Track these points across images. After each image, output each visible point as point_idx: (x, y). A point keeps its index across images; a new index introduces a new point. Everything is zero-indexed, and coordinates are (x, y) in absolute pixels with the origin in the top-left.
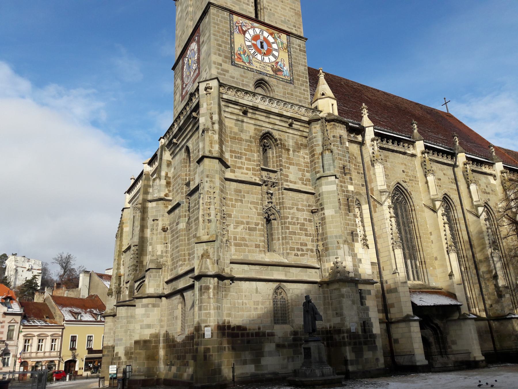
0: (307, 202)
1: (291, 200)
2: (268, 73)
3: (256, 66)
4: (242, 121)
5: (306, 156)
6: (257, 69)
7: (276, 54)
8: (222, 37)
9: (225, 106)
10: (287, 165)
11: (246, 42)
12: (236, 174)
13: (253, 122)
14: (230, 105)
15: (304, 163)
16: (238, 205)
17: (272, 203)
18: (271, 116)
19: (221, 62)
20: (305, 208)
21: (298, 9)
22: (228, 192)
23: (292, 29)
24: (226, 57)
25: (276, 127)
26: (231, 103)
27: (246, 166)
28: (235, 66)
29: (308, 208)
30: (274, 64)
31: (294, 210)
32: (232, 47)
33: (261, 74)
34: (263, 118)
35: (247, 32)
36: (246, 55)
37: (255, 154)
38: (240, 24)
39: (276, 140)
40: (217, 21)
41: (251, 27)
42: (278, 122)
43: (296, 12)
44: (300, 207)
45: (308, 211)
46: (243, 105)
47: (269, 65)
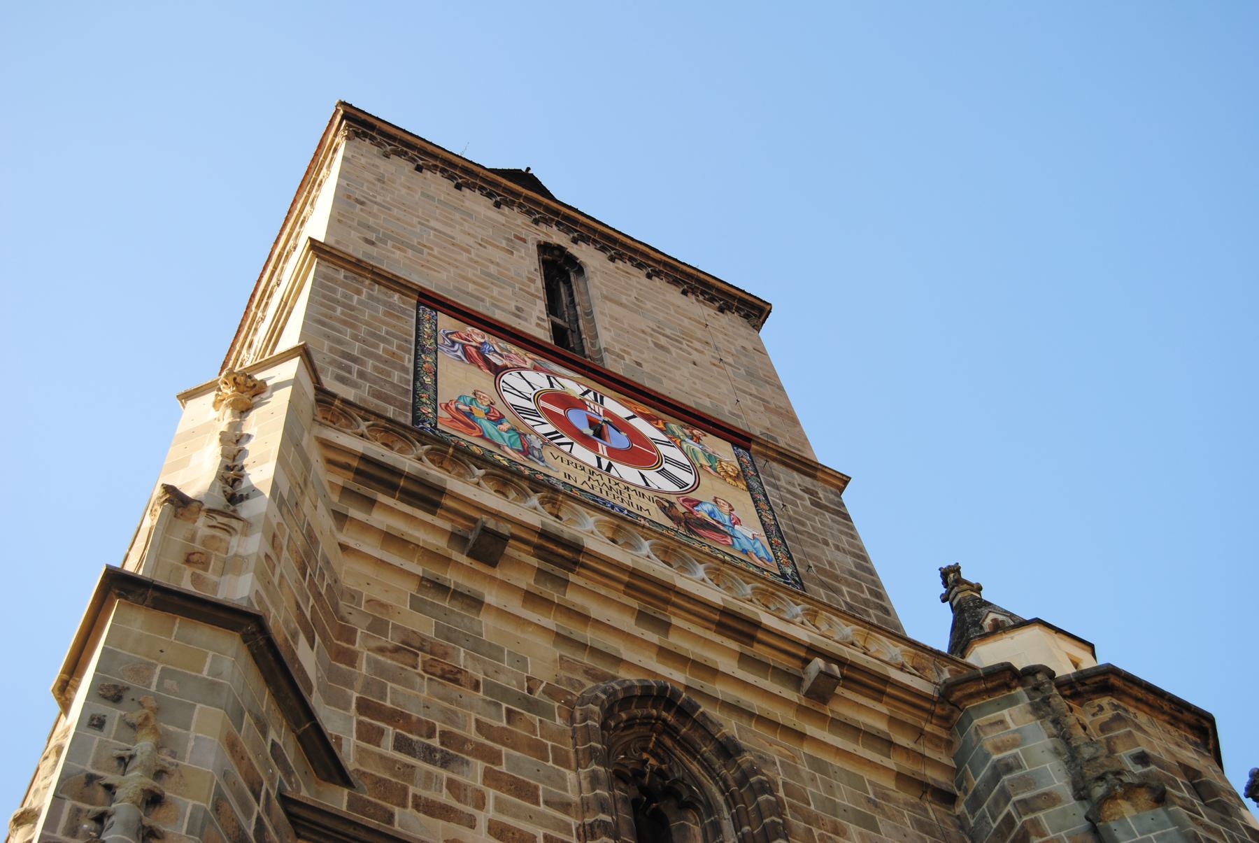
2: (645, 514)
4: (475, 603)
6: (572, 482)
9: (345, 492)
11: (504, 393)
14: (382, 498)
25: (720, 689)
26: (391, 488)
30: (673, 499)
32: (423, 384)
34: (627, 623)
37: (570, 775)
38: (474, 344)
39: (729, 750)
41: (535, 369)
46: (469, 513)
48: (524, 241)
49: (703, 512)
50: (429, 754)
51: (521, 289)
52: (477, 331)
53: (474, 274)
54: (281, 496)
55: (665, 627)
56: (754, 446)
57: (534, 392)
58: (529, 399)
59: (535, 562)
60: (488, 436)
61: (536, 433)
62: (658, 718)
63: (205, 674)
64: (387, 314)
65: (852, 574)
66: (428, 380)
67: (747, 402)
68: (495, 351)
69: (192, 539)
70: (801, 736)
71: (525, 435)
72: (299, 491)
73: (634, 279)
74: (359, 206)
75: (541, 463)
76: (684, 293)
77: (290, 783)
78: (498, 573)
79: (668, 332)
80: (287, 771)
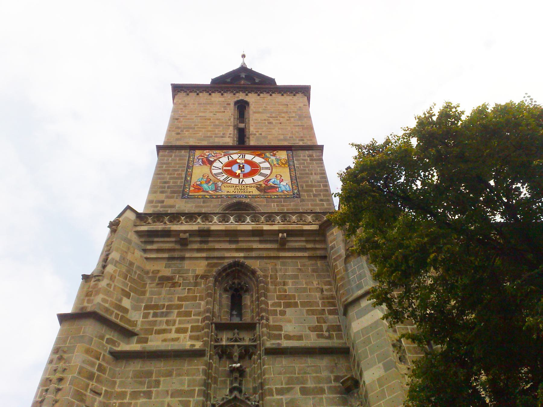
0: (332, 372)
1: (285, 373)
2: (251, 194)
3: (225, 191)
5: (325, 287)
6: (229, 194)
7: (268, 172)
8: (171, 174)
9: (146, 242)
10: (278, 309)
12: (149, 343)
13: (204, 255)
14: (156, 239)
15: (323, 298)
16: (136, 404)
17: (240, 391)
18: (240, 239)
19: (163, 199)
20: (325, 386)
21: (307, 124)
22: (118, 381)
23: (297, 143)
24: (173, 192)
25: (254, 254)
27: (177, 325)
28: (188, 198)
29: (333, 384)
30: (261, 183)
31: (296, 394)
32: (187, 181)
33: (236, 197)
35: (217, 161)
36: (210, 184)
38: (206, 156)
40: (168, 160)
41: (224, 156)
42: (255, 246)
43: (305, 126)
44: (310, 385)
45: (332, 390)
47: (253, 185)
48: (229, 104)
49: (271, 183)
50: (163, 315)
51: (225, 125)
52: (207, 151)
53: (211, 128)
54: (117, 262)
55: (237, 242)
56: (293, 149)
57: (222, 165)
58: (220, 169)
59: (198, 239)
60: (205, 190)
61: (221, 181)
62: (236, 269)
63: (81, 334)
64: (180, 160)
65: (318, 182)
66: (189, 178)
67: (297, 129)
68: (213, 156)
69: (89, 288)
70: (278, 258)
71: (217, 183)
72: (125, 254)
73: (265, 99)
74: (176, 121)
75: (220, 191)
76: (282, 95)
77: (115, 346)
78: (189, 247)
79: (274, 115)
80: (113, 342)
